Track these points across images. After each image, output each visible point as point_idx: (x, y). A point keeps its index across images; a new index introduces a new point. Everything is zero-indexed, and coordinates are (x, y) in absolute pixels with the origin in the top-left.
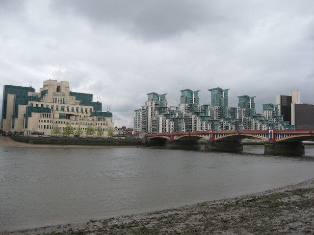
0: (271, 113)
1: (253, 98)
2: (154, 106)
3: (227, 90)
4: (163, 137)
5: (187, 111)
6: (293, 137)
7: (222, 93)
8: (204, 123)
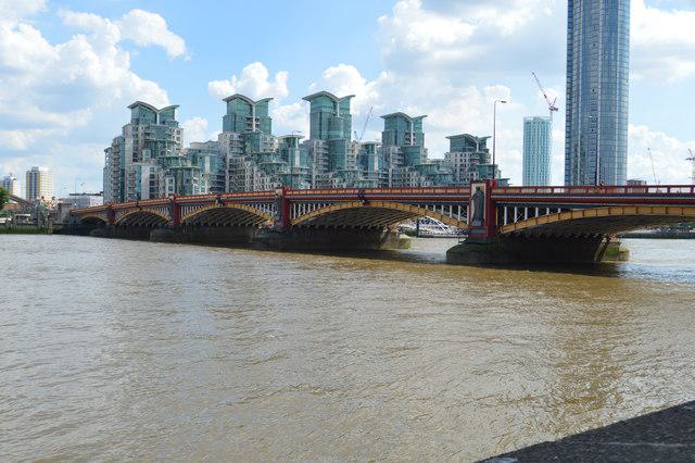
0: (468, 158)
1: (418, 120)
2: (141, 138)
3: (349, 98)
4: (96, 216)
5: (236, 150)
6: (327, 210)
7: (335, 108)
8: (267, 179)
